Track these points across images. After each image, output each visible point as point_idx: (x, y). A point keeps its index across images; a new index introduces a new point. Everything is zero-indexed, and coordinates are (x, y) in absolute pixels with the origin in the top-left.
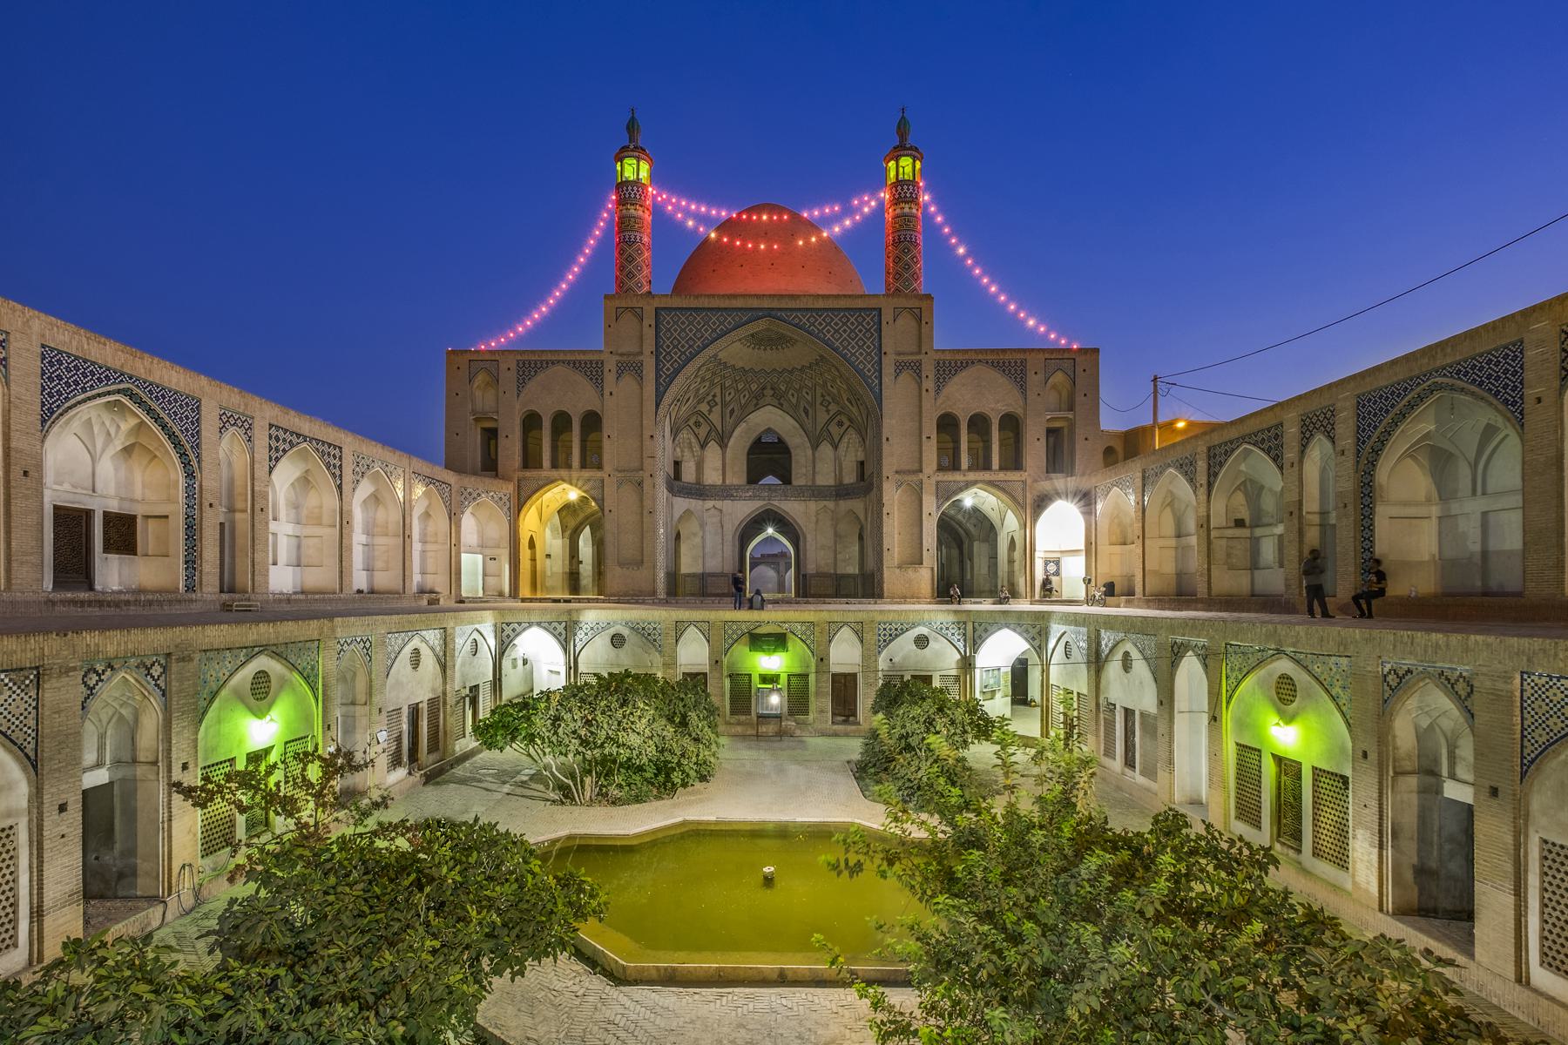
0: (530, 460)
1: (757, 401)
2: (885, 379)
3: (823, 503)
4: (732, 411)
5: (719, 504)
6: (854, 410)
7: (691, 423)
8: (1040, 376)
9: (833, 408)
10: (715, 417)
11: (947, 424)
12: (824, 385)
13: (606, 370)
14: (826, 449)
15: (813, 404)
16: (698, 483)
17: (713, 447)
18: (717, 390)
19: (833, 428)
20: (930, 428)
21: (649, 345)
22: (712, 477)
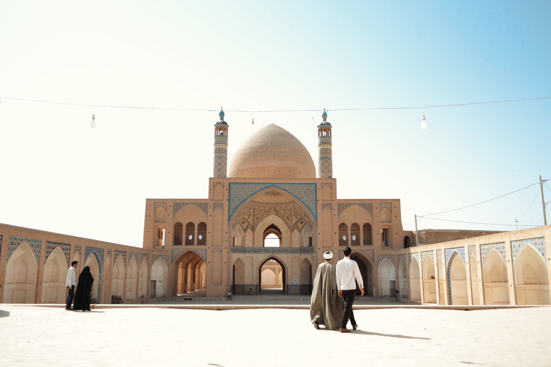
0: (177, 241)
2: (318, 210)
3: (294, 255)
4: (257, 218)
5: (251, 255)
6: (307, 219)
7: (240, 222)
8: (378, 209)
9: (299, 217)
10: (250, 220)
11: (343, 226)
12: (295, 209)
14: (296, 232)
15: (291, 215)
16: (242, 246)
17: (249, 231)
18: (252, 210)
19: (299, 224)
20: (336, 229)
22: (249, 244)
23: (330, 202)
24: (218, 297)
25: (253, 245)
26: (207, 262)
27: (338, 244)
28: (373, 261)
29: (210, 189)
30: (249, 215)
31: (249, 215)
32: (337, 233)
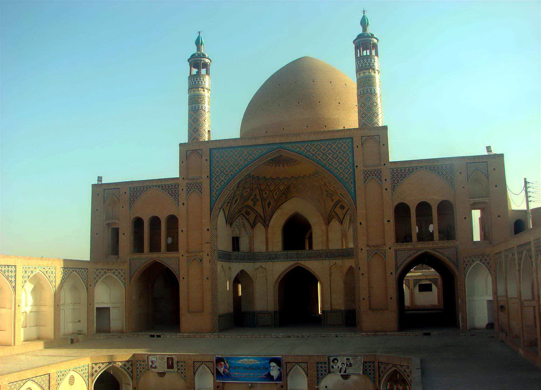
0: (138, 245)
1: (286, 195)
3: (333, 262)
4: (269, 204)
5: (264, 265)
13: (180, 190)
14: (335, 224)
17: (259, 227)
19: (338, 210)
20: (390, 214)
21: (206, 173)
22: (260, 246)
23: (379, 168)
24: (198, 332)
25: (267, 248)
26: (181, 278)
27: (393, 240)
28: (457, 266)
29: (181, 162)
30: (255, 201)
31: (255, 201)
32: (392, 220)
